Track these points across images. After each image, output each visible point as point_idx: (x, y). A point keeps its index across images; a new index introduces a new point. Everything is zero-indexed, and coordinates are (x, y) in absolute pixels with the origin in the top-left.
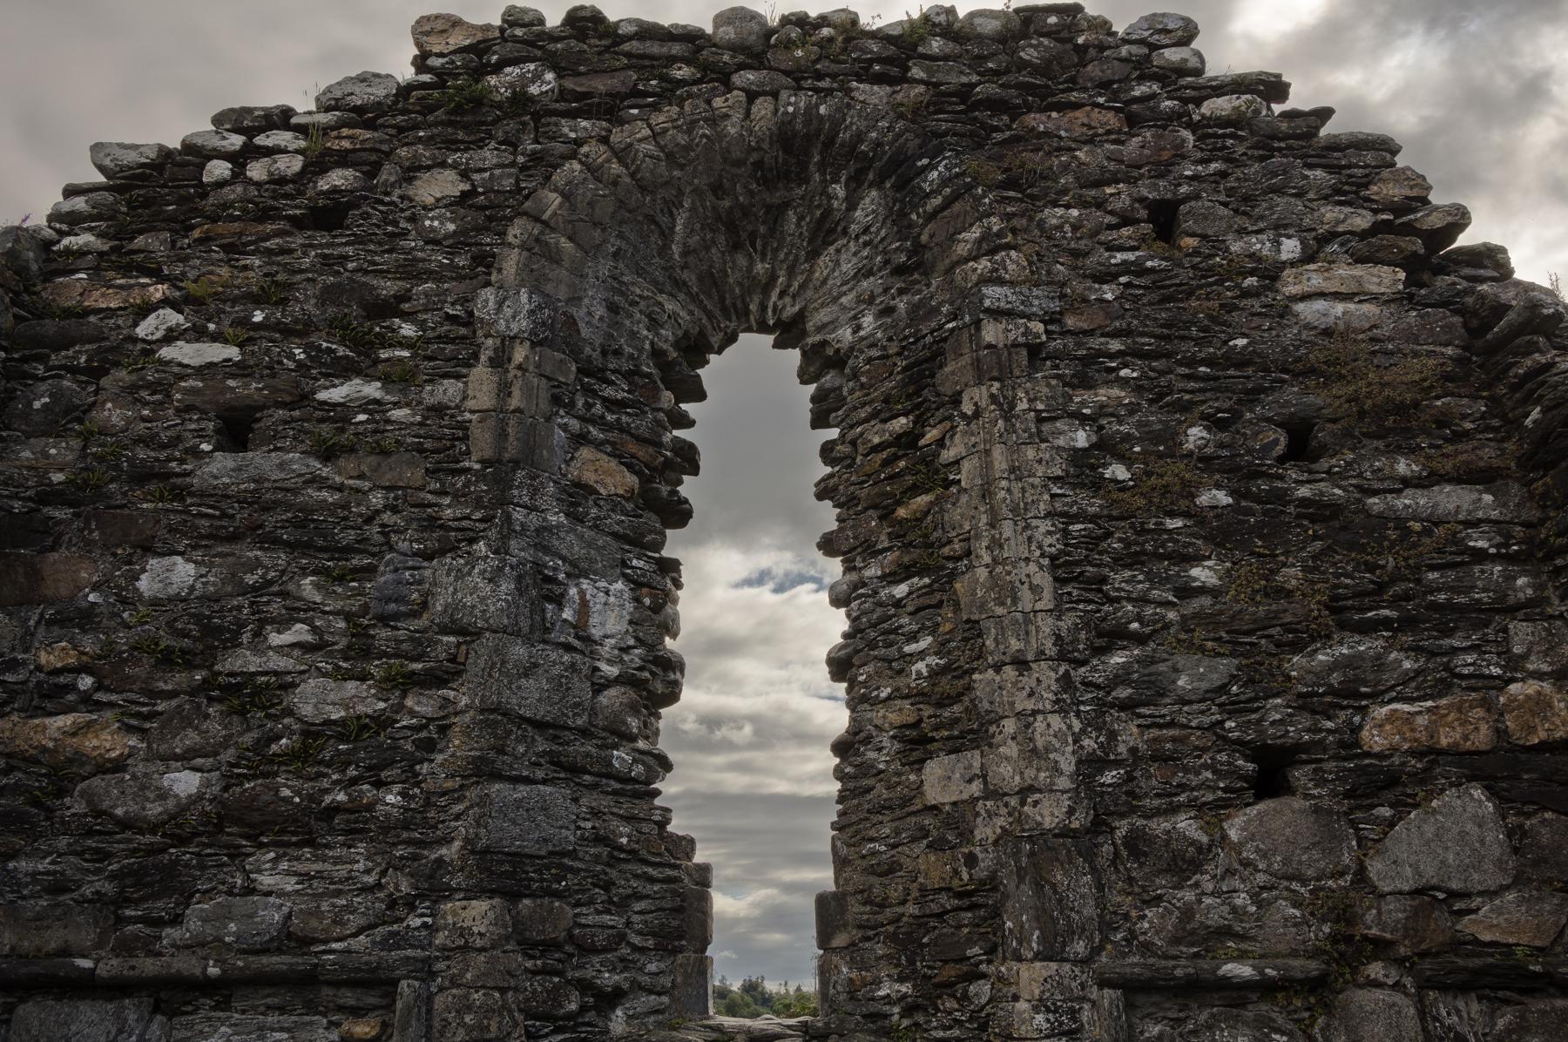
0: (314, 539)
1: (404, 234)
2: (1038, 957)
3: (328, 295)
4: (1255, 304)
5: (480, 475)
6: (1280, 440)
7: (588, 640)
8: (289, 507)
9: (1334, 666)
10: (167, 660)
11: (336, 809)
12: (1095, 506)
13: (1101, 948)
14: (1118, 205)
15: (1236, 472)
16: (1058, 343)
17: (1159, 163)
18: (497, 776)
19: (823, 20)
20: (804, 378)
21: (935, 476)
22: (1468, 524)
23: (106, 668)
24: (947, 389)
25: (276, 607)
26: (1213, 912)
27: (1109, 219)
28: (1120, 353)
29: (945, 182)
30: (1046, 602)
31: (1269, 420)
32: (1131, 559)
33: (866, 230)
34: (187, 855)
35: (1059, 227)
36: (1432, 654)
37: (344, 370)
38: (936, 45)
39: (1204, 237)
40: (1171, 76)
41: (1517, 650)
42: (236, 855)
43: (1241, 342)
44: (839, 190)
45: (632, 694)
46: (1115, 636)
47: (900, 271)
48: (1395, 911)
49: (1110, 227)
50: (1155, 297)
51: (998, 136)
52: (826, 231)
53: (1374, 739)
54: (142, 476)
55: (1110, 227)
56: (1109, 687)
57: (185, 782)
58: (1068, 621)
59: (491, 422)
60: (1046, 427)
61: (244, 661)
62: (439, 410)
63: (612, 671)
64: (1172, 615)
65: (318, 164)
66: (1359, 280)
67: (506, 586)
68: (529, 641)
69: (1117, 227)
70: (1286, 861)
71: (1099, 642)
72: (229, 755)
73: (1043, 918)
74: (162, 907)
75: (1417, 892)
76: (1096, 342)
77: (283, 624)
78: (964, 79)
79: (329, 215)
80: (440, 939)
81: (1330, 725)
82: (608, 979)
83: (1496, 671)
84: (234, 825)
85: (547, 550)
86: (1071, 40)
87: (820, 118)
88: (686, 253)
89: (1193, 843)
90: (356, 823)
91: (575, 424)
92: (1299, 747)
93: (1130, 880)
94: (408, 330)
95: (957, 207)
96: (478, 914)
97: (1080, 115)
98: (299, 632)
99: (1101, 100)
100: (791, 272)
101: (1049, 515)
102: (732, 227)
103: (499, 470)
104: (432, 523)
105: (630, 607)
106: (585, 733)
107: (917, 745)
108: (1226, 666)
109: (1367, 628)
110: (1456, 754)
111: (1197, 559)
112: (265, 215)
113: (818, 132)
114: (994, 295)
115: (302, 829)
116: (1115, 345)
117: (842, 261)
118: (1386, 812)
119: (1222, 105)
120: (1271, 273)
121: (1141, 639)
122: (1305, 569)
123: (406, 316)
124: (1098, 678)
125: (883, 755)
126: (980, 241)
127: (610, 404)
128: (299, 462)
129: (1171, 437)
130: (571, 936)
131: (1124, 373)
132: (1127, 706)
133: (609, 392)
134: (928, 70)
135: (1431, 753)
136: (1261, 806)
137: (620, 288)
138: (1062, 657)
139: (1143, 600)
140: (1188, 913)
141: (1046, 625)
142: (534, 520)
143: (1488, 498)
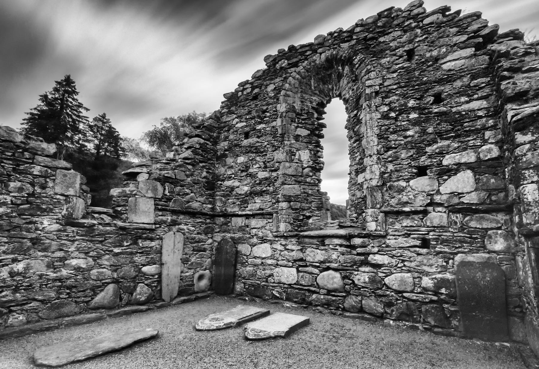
1: (266, 98)
2: (371, 208)
4: (431, 68)
5: (280, 137)
6: (432, 99)
7: (301, 161)
8: (254, 147)
9: (436, 149)
10: (242, 171)
11: (264, 191)
12: (387, 122)
13: (382, 206)
14: (399, 54)
15: (419, 109)
16: (382, 90)
17: (410, 40)
18: (285, 184)
19: (335, 32)
22: (478, 110)
23: (236, 174)
24: (361, 104)
25: (254, 162)
26: (405, 199)
27: (398, 58)
28: (396, 88)
29: (359, 61)
30: (376, 143)
31: (430, 96)
33: (347, 74)
34: (247, 198)
35: (385, 63)
36: (462, 142)
38: (358, 29)
39: (421, 55)
41: (486, 138)
42: (253, 198)
43: (425, 79)
44: (340, 68)
45: (310, 169)
46: (389, 149)
47: (354, 81)
48: (445, 197)
49: (397, 59)
50: (406, 73)
51: (372, 46)
52: (340, 76)
53: (445, 162)
55: (397, 59)
56: (387, 159)
58: (380, 146)
59: (281, 128)
60: (378, 108)
61: (251, 170)
62: (273, 127)
63: (305, 166)
64: (402, 142)
66: (460, 54)
67: (285, 154)
68: (290, 162)
69: (399, 59)
70: (422, 189)
71: (386, 150)
72: (251, 184)
73: (372, 202)
74: (246, 205)
75: (451, 193)
76: (390, 87)
77: (255, 164)
78: (365, 35)
80: (279, 208)
81: (435, 160)
82: (308, 214)
83: (479, 144)
85: (291, 147)
86: (390, 16)
87: (334, 55)
88: (315, 87)
89: (402, 186)
90: (267, 192)
91: (296, 125)
92: (427, 166)
93: (390, 194)
94: (268, 114)
95: (362, 65)
96: (284, 205)
97: (392, 35)
98: (257, 166)
99: (397, 29)
100: (336, 86)
101: (377, 126)
102: (323, 81)
103: (282, 135)
104: (274, 146)
105: (309, 154)
106: (301, 176)
107: (357, 173)
108: (412, 152)
109: (447, 139)
110: (465, 164)
111: (408, 130)
113: (334, 57)
114: (368, 83)
116: (395, 87)
117: (344, 82)
118: (446, 177)
121: (395, 148)
122: (434, 128)
123: (267, 112)
124: (386, 157)
126: (366, 71)
127: (303, 119)
128: (256, 139)
129: (405, 105)
130: (300, 208)
131: (397, 92)
132: (391, 162)
133: (302, 117)
134: (357, 36)
135: (459, 164)
136: (418, 178)
137: (303, 97)
138: (378, 154)
139: (396, 140)
140: (400, 199)
141: (375, 148)
142: (289, 143)
143: (485, 102)
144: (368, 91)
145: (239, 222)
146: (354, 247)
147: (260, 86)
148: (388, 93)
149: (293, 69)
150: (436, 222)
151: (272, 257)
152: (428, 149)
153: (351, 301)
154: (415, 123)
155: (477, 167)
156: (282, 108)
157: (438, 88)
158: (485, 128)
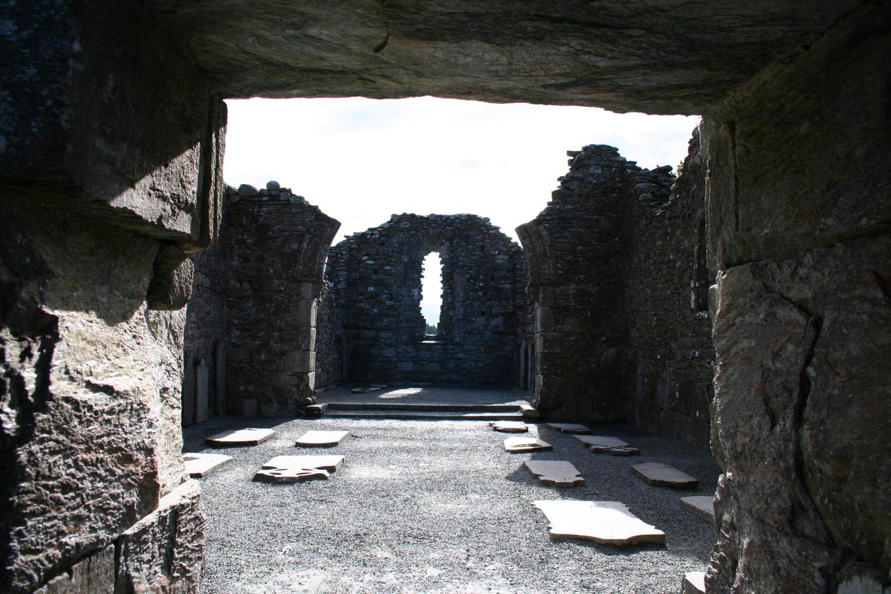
52: (442, 244)
57: (375, 311)
79: (382, 244)
112: (375, 243)
115: (388, 316)
117: (444, 248)
125: (445, 309)
144: (460, 263)
147: (387, 236)
148: (470, 268)
151: (397, 356)
154: (482, 288)
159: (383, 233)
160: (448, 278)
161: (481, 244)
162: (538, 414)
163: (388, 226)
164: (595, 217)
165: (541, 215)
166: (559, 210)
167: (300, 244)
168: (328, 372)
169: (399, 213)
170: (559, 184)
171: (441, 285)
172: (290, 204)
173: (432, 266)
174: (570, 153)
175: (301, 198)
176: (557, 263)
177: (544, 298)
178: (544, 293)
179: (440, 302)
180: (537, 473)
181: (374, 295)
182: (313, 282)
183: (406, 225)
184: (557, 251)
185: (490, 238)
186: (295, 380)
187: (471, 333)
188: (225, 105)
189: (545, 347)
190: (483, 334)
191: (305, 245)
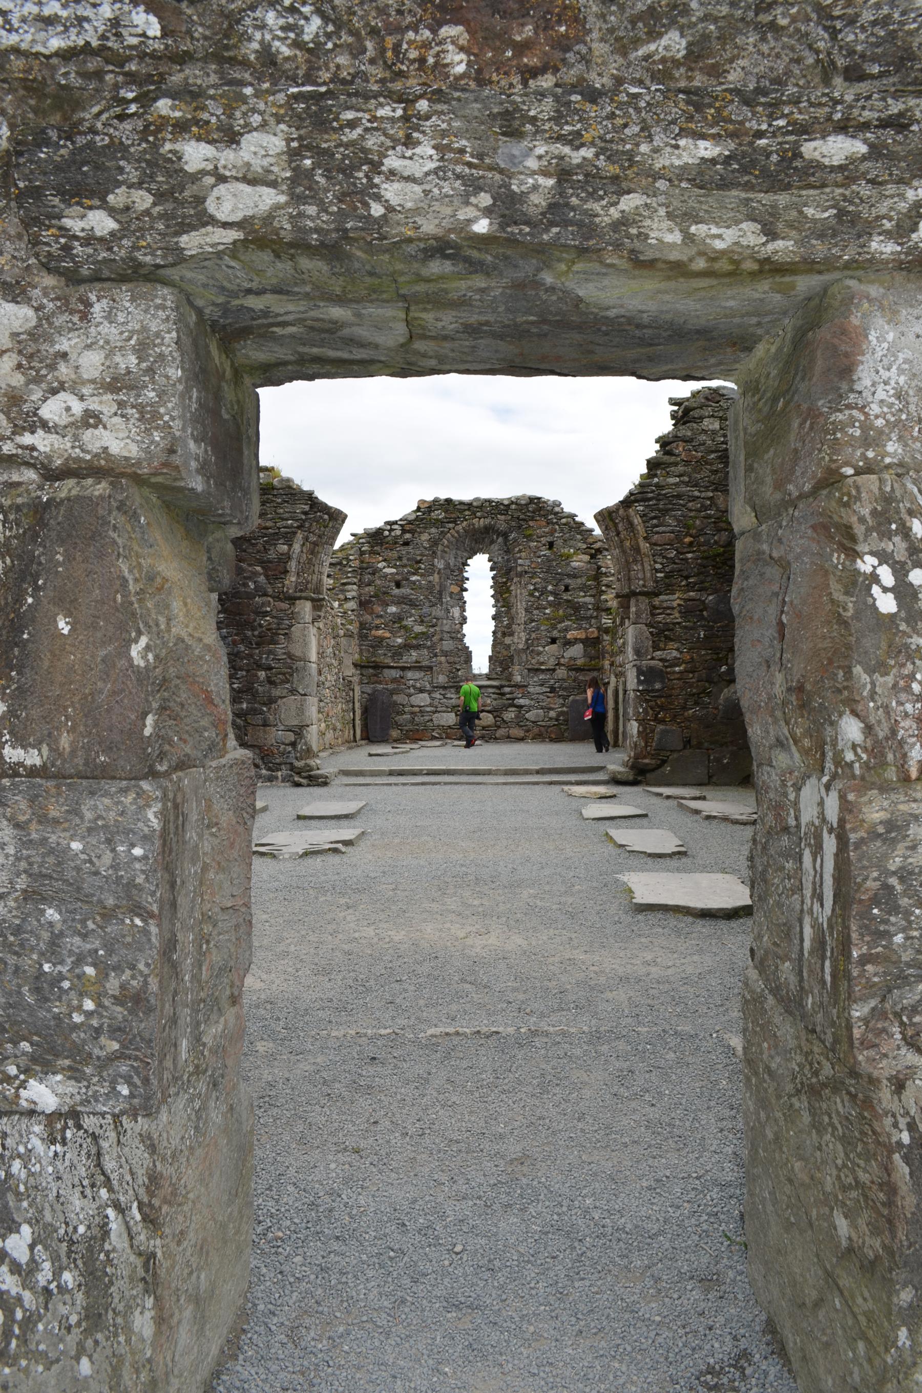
0: (413, 604)
3: (408, 559)
20: (490, 560)
21: (508, 591)
26: (542, 660)
32: (537, 608)
37: (414, 574)
38: (513, 507)
40: (556, 514)
46: (533, 621)
52: (492, 542)
54: (384, 593)
65: (404, 531)
79: (406, 544)
84: (407, 647)
107: (504, 634)
112: (396, 543)
114: (520, 561)
115: (417, 647)
117: (495, 547)
119: (564, 521)
120: (568, 557)
125: (499, 635)
129: (546, 587)
135: (576, 639)
144: (519, 569)
145: (395, 674)
146: (503, 694)
149: (451, 525)
150: (560, 676)
151: (431, 705)
152: (559, 626)
153: (501, 732)
154: (550, 604)
155: (586, 642)
156: (440, 565)
157: (568, 581)
158: (592, 617)
159: (407, 528)
160: (501, 591)
161: (549, 539)
162: (631, 778)
163: (413, 517)
164: (711, 494)
165: (631, 494)
166: (657, 485)
167: (290, 546)
168: (335, 730)
169: (429, 498)
170: (657, 447)
171: (492, 601)
172: (273, 488)
173: (479, 571)
174: (673, 402)
175: (289, 480)
176: (656, 562)
177: (638, 614)
178: (637, 605)
179: (492, 625)
180: (624, 843)
181: (398, 619)
182: (313, 600)
183: (439, 514)
184: (655, 544)
185: (562, 531)
186: (291, 737)
187: (537, 670)
188: (257, 395)
189: (640, 682)
190: (554, 670)
191: (297, 547)
